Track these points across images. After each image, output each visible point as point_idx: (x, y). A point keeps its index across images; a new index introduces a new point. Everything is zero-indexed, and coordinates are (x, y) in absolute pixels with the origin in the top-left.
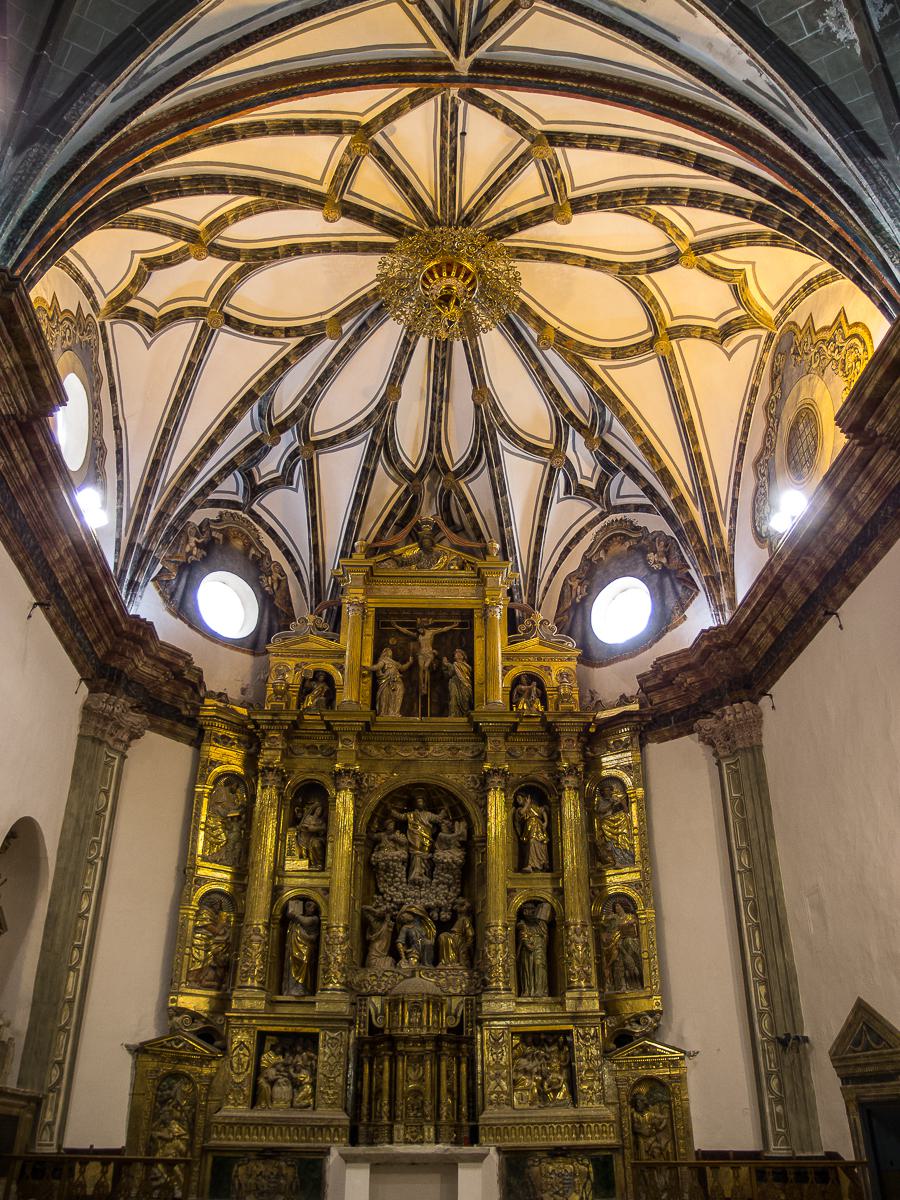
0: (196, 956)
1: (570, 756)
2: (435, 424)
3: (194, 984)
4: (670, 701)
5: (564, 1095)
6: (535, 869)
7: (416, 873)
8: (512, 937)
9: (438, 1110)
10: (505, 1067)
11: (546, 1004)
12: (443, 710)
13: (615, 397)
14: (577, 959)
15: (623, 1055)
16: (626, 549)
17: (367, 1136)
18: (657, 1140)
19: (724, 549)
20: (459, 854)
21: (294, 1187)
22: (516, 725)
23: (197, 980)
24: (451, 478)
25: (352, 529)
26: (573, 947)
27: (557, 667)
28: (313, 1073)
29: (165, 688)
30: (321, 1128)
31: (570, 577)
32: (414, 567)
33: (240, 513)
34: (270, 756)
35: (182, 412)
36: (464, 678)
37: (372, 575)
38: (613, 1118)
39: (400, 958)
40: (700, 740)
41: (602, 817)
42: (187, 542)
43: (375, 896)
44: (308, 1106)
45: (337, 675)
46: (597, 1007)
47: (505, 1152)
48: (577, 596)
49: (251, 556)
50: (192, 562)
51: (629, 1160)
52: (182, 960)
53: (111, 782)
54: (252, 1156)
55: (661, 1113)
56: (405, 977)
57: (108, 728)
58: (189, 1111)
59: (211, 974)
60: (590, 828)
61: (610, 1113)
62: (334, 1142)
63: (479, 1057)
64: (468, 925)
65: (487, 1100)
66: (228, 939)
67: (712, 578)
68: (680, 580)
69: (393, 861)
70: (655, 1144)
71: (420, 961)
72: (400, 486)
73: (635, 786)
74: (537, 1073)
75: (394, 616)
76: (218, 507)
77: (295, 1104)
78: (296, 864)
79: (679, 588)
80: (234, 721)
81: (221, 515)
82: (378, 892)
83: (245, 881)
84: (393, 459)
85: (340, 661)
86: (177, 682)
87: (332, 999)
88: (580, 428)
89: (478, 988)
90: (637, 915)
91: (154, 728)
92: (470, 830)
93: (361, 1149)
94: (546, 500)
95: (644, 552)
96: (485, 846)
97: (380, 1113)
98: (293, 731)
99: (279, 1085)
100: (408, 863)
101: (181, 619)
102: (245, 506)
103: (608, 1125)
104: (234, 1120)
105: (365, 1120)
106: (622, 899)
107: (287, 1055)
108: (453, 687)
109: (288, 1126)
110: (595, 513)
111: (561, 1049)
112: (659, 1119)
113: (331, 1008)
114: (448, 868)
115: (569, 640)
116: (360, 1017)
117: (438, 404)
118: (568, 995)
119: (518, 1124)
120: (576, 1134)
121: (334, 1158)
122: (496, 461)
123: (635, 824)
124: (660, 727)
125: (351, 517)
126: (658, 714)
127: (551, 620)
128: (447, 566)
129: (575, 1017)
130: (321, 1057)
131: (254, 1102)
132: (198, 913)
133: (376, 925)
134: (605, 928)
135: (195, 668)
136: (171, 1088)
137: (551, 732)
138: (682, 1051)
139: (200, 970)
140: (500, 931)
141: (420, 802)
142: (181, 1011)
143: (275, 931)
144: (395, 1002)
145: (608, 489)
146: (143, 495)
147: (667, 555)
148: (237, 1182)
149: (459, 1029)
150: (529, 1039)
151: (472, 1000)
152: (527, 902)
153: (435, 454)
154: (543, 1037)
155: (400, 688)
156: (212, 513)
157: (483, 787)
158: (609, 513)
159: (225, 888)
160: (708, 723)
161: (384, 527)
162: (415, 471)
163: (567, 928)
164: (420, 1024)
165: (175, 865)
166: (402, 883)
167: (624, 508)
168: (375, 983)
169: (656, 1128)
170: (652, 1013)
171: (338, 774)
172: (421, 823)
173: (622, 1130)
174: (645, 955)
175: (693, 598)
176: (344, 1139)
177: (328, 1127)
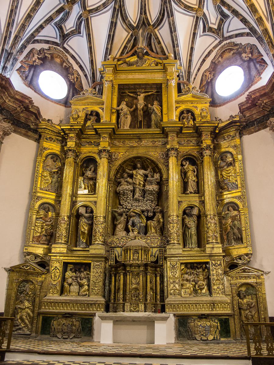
0: (37, 230)
1: (207, 141)
3: (36, 242)
4: (254, 114)
6: (191, 193)
7: (137, 195)
8: (180, 223)
9: (146, 297)
10: (177, 278)
11: (197, 251)
12: (149, 126)
14: (211, 230)
15: (233, 273)
16: (231, 54)
17: (113, 308)
18: (250, 312)
20: (157, 187)
21: (79, 330)
22: (181, 128)
23: (38, 240)
24: (151, 27)
25: (108, 51)
26: (209, 225)
27: (200, 106)
28: (89, 280)
29: (21, 115)
30: (91, 304)
31: (205, 71)
32: (135, 66)
33: (59, 48)
34: (71, 144)
36: (158, 111)
37: (117, 70)
38: (229, 301)
39: (130, 232)
40: (270, 130)
41: (222, 169)
42: (33, 56)
43: (119, 206)
44: (86, 295)
45: (100, 111)
46: (221, 252)
47: (177, 316)
48: (208, 79)
50: (36, 65)
51: (237, 321)
54: (60, 316)
55: (252, 299)
56: (132, 240)
58: (32, 297)
61: (228, 299)
62: (98, 311)
63: (166, 274)
64: (160, 217)
66: (52, 223)
68: (258, 62)
70: (249, 314)
71: (139, 233)
72: (129, 33)
74: (193, 281)
75: (127, 88)
76: (48, 44)
78: (83, 191)
79: (258, 66)
81: (50, 47)
82: (120, 204)
83: (60, 199)
84: (125, 18)
86: (27, 112)
87: (97, 249)
89: (165, 244)
90: (239, 211)
91: (15, 131)
92: (161, 177)
93: (110, 314)
94: (194, 34)
95: (240, 54)
96: (168, 183)
97: (119, 298)
98: (81, 134)
99: (73, 285)
100: (134, 191)
101: (31, 88)
103: (227, 305)
104: (52, 301)
105: (112, 301)
106: (232, 205)
107: (77, 273)
108: (153, 116)
109: (77, 304)
110: (217, 42)
111: (204, 270)
112: (251, 302)
113: (98, 252)
114: (151, 193)
115: (205, 95)
116: (111, 257)
118: (207, 246)
119: (184, 304)
120: (211, 308)
121: (96, 319)
122: (171, 14)
124: (249, 127)
125: (107, 46)
128: (150, 65)
129: (211, 256)
130: (92, 274)
131: (62, 292)
132: (38, 212)
133: (118, 217)
134: (224, 217)
135: (35, 106)
136: (24, 287)
137: (198, 132)
139: (39, 236)
140: (175, 218)
141: (139, 165)
142: (29, 254)
143: (73, 220)
144: (126, 250)
145: (223, 28)
146: (7, 27)
147: (252, 53)
148: (53, 327)
149: (157, 262)
150: (189, 266)
151: (162, 250)
152: (187, 207)
153: (143, 16)
154: (195, 265)
155: (129, 117)
156: (46, 46)
157: (167, 156)
158: (223, 41)
159: (52, 202)
161: (122, 53)
162: (135, 25)
163: (206, 216)
164: (138, 259)
166: (130, 200)
167: (230, 37)
168: (118, 242)
169: (249, 306)
170: (247, 255)
171: (100, 152)
172: (139, 174)
173: (233, 307)
174: (244, 229)
176: (102, 309)
177: (95, 304)
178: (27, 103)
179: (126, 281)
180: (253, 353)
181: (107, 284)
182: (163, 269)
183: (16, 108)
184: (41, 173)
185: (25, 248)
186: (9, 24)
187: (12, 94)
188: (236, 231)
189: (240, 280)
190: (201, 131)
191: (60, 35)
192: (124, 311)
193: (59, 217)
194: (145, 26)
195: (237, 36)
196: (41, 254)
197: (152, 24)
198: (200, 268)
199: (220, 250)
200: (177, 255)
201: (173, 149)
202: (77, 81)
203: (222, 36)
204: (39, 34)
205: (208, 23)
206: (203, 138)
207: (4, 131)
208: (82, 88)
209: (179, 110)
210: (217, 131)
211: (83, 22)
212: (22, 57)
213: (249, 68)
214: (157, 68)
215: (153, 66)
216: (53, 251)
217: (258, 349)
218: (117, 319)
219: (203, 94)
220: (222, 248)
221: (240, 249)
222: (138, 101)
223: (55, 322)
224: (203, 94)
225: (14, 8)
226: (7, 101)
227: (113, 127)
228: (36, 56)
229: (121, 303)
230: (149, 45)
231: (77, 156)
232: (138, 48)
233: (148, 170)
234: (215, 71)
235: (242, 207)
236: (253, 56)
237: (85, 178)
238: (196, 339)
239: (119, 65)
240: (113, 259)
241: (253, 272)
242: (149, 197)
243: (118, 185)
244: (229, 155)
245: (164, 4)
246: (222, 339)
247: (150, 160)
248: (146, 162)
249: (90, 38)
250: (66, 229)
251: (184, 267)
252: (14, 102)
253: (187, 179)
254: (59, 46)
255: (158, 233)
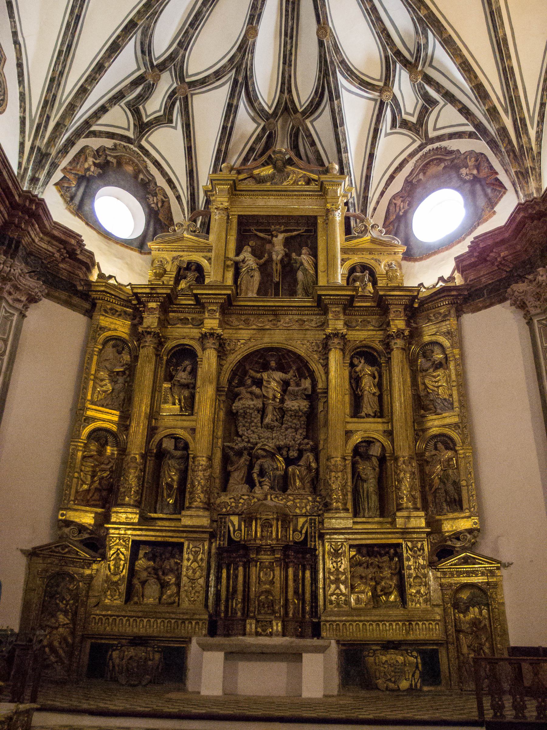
2: (287, 66)
5: (395, 596)
10: (344, 573)
12: (293, 293)
13: (439, 22)
19: (532, 149)
22: (352, 297)
24: (299, 115)
26: (402, 475)
29: (61, 265)
31: (394, 197)
32: (269, 184)
33: (132, 146)
35: (73, 37)
37: (236, 190)
40: (511, 305)
42: (86, 160)
43: (235, 438)
44: (174, 602)
45: (205, 263)
46: (424, 525)
47: (344, 645)
48: (400, 210)
49: (139, 180)
50: (90, 176)
52: (71, 482)
53: (10, 332)
57: (8, 287)
59: (96, 496)
60: (414, 383)
63: (321, 566)
64: (311, 460)
65: (327, 600)
66: (112, 467)
67: (522, 173)
69: (249, 408)
71: (272, 488)
72: (259, 124)
73: (452, 346)
77: (162, 600)
79: (489, 191)
80: (123, 297)
81: (115, 145)
82: (238, 435)
83: (128, 423)
84: (252, 99)
85: (209, 254)
88: (406, 63)
90: (456, 451)
91: (48, 296)
95: (456, 168)
96: (327, 397)
99: (149, 585)
100: (263, 412)
102: (135, 140)
103: (434, 623)
105: (222, 615)
108: (300, 275)
114: (296, 414)
115: (394, 239)
116: (221, 532)
117: (289, 47)
118: (398, 514)
119: (355, 621)
121: (194, 647)
123: (454, 377)
126: (473, 290)
127: (381, 223)
128: (296, 183)
129: (405, 532)
130: (185, 563)
133: (234, 459)
134: (428, 462)
135: (87, 251)
138: (499, 562)
139: (88, 491)
141: (273, 364)
142: (68, 523)
143: (152, 462)
146: (43, 108)
147: (478, 167)
148: (111, 664)
150: (364, 551)
151: (315, 520)
153: (286, 95)
155: (257, 276)
156: (109, 143)
158: (427, 144)
159: (114, 428)
160: (520, 287)
161: (246, 160)
163: (396, 459)
165: (70, 406)
167: (439, 138)
170: (470, 531)
171: (204, 336)
174: (464, 483)
175: (502, 196)
178: (73, 245)
179: (249, 578)
180: (489, 715)
181: (212, 583)
182: (316, 557)
183: (54, 254)
184: (93, 372)
185: (61, 512)
186: (46, 102)
187: (47, 229)
188: (450, 488)
189: (458, 579)
190: (388, 304)
191: (135, 125)
192: (244, 634)
193: (126, 456)
194: (289, 113)
195: (451, 136)
196: (90, 525)
197: (300, 110)
198: (385, 555)
199: (421, 523)
200: (343, 531)
201: (336, 335)
202: (162, 207)
203: (425, 137)
204: (99, 122)
205: (400, 112)
206: (391, 316)
207: (30, 295)
208: (171, 220)
209: (348, 264)
210: (416, 305)
211: (178, 103)
212: (64, 163)
213: (473, 193)
214: (307, 187)
215: (302, 185)
216: (113, 519)
217: (498, 708)
218: (234, 650)
219: (390, 238)
220: (426, 519)
221: (457, 521)
222: (273, 245)
223: (114, 653)
224: (390, 238)
225: (57, 76)
226: (36, 240)
227: (229, 292)
228: (91, 160)
229: (241, 620)
230: (295, 147)
231: (161, 344)
232: (274, 152)
233: (289, 372)
234: (413, 198)
235: (461, 444)
236: (481, 174)
237: (174, 385)
238: (378, 689)
239: (240, 181)
240: (224, 536)
241: (482, 564)
242: (291, 422)
243: (235, 398)
244: (437, 349)
245: (324, 77)
246: (425, 689)
247: (294, 354)
248: (287, 357)
249: (190, 132)
250: (138, 478)
251: (354, 553)
252: (49, 242)
253: (361, 391)
254: (132, 144)
255: (307, 490)
